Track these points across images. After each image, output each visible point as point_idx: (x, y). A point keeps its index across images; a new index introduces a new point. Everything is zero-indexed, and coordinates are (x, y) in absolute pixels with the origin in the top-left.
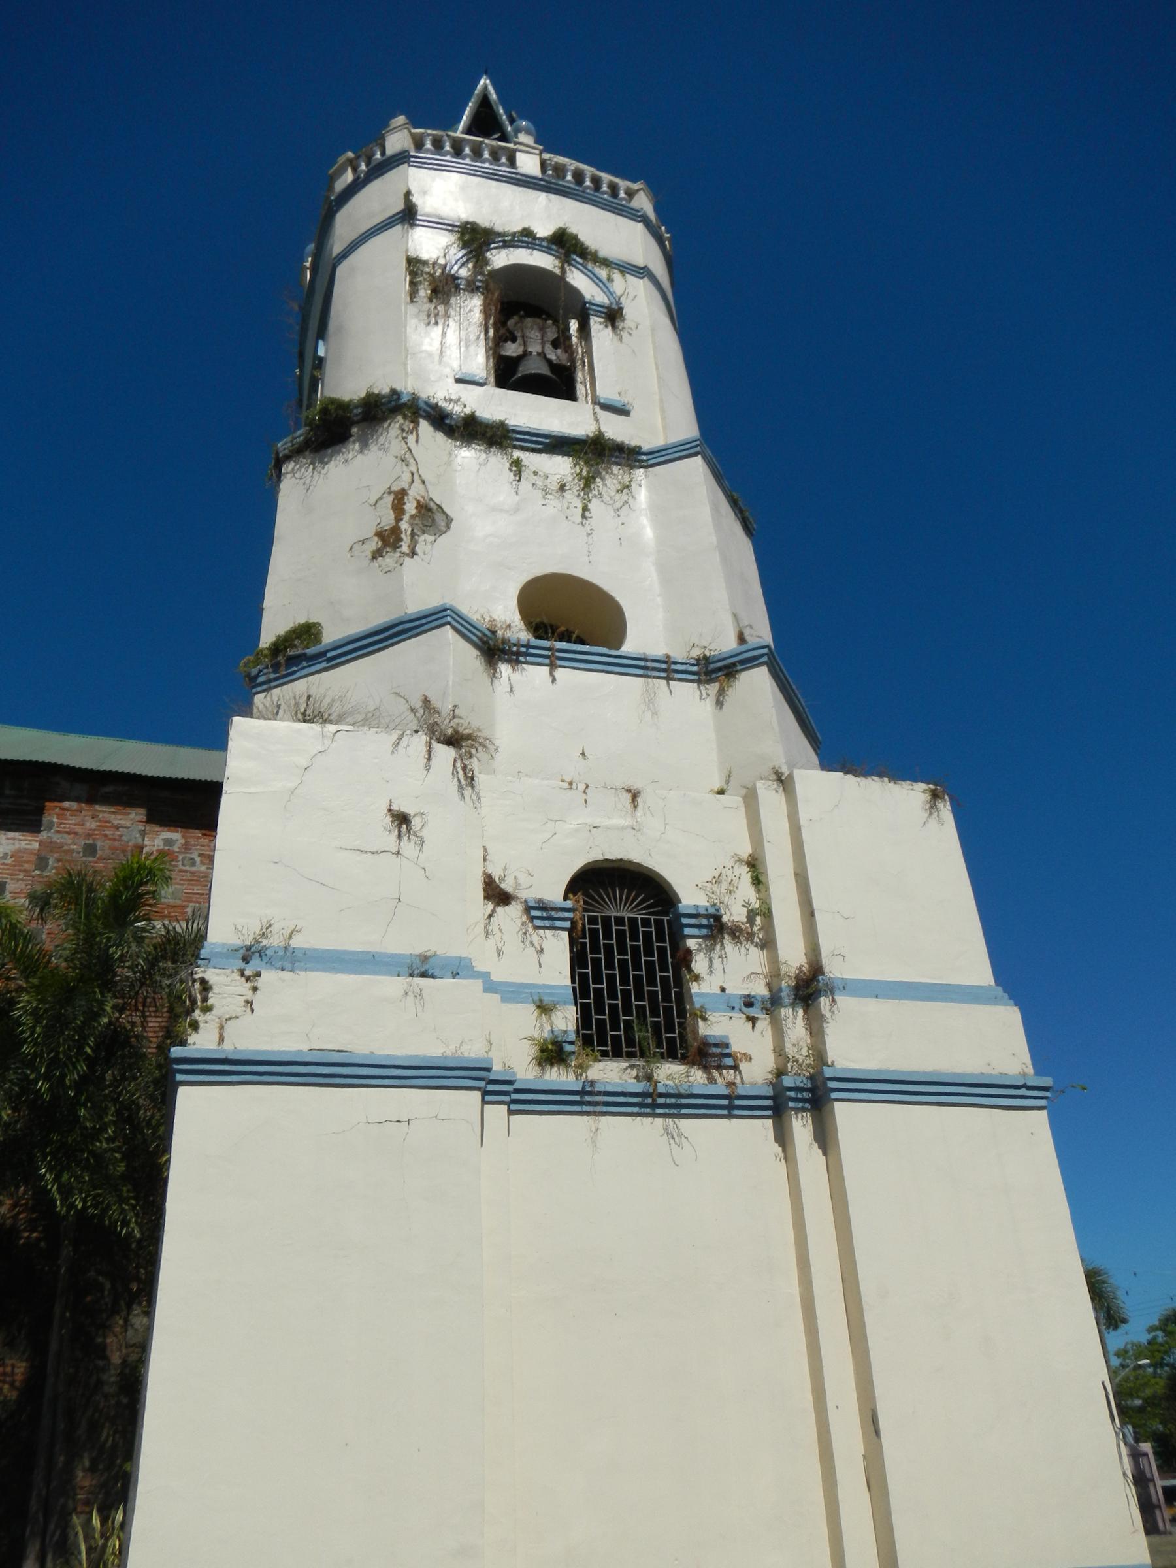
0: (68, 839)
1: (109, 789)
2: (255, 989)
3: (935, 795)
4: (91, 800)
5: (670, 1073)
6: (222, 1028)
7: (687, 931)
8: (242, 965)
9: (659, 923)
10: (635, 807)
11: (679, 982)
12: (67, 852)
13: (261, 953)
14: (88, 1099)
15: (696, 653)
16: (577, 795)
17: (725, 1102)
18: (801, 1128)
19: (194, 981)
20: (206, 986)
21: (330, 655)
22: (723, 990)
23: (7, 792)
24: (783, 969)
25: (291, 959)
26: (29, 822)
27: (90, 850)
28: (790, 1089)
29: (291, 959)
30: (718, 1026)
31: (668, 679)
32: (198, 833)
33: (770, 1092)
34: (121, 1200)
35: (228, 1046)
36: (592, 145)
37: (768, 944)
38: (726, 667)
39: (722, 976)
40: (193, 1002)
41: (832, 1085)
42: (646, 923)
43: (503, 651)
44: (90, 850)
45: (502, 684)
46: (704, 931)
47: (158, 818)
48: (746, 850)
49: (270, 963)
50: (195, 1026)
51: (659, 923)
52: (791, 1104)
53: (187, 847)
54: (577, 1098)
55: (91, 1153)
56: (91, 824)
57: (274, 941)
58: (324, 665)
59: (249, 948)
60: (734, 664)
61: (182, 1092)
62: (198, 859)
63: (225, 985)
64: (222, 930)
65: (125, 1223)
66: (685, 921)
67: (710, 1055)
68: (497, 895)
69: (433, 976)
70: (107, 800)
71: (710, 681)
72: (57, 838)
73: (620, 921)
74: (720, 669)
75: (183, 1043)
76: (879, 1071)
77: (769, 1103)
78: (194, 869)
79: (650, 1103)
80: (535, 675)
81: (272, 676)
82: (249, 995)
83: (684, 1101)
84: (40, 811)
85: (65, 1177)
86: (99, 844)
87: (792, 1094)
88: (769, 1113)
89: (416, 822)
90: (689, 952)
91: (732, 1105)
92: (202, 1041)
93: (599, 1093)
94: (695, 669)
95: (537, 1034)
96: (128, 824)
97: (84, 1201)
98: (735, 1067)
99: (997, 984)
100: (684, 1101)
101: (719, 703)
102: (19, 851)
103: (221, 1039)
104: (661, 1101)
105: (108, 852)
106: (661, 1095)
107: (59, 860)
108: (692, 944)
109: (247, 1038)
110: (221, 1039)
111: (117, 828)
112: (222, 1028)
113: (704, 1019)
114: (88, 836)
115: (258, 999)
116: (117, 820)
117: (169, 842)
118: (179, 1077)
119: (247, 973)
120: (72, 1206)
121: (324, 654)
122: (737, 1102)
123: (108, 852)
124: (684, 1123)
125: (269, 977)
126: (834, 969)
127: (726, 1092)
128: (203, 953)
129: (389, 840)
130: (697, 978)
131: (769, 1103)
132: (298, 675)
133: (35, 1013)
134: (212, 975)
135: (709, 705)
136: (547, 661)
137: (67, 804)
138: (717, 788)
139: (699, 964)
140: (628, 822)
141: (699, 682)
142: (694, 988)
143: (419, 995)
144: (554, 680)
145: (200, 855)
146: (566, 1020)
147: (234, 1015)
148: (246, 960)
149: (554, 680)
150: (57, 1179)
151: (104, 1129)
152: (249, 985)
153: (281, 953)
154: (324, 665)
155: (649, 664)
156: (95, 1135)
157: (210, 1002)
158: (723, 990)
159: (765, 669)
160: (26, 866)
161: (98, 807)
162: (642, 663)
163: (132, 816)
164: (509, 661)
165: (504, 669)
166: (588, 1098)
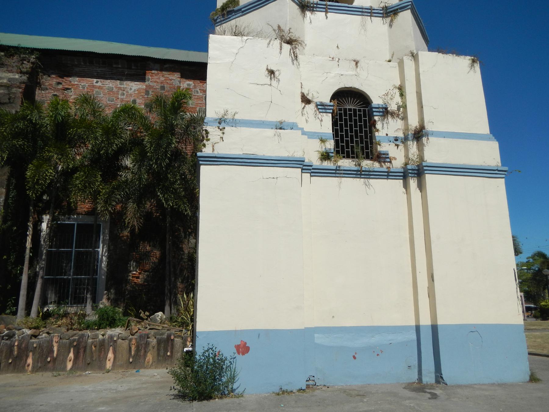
0: (155, 84)
2: (223, 133)
3: (474, 61)
4: (161, 70)
5: (367, 164)
6: (213, 146)
7: (375, 114)
8: (219, 125)
9: (364, 111)
11: (371, 132)
12: (155, 89)
14: (170, 172)
15: (382, 5)
16: (335, 63)
17: (386, 174)
18: (413, 183)
20: (207, 132)
21: (243, 10)
22: (387, 135)
23: (133, 67)
24: (410, 127)
25: (235, 123)
26: (141, 78)
27: (163, 88)
28: (410, 170)
29: (235, 123)
30: (384, 147)
31: (371, 16)
32: (198, 82)
33: (402, 171)
34: (184, 203)
35: (215, 152)
37: (405, 118)
38: (394, 10)
39: (386, 130)
40: (203, 137)
41: (425, 168)
42: (360, 111)
43: (308, 6)
44: (163, 88)
45: (307, 20)
46: (381, 114)
47: (185, 76)
48: (398, 83)
49: (228, 124)
50: (204, 145)
51: (364, 111)
52: (410, 175)
53: (195, 87)
54: (334, 172)
55: (173, 188)
56: (162, 79)
57: (229, 117)
58: (241, 14)
59: (220, 119)
60: (397, 9)
61: (202, 167)
62: (199, 91)
63: (213, 132)
64: (211, 113)
65: (186, 211)
66: (374, 110)
67: (381, 158)
68: (306, 100)
69: (284, 129)
70: (167, 70)
71: (387, 17)
72: (151, 84)
73: (350, 110)
74: (391, 12)
75: (201, 151)
76: (443, 164)
77: (402, 174)
79: (360, 173)
80: (320, 15)
81: (222, 19)
83: (371, 173)
84: (145, 74)
85: (166, 196)
86: (165, 86)
87: (411, 171)
88: (402, 178)
89: (277, 73)
90: (375, 121)
91: (388, 175)
92: (207, 151)
93: (342, 170)
94: (382, 12)
95: (320, 150)
96: (175, 78)
97: (173, 203)
98: (390, 162)
99: (491, 133)
100: (371, 173)
101: (391, 26)
102: (139, 89)
104: (363, 173)
105: (169, 89)
106: (363, 171)
108: (376, 118)
109: (222, 150)
111: (171, 80)
112: (213, 146)
113: (380, 145)
114: (162, 83)
115: (225, 137)
116: (171, 77)
117: (189, 85)
118: (201, 162)
119: (220, 128)
120: (169, 205)
121: (240, 9)
122: (390, 174)
124: (371, 181)
125: (228, 129)
126: (429, 127)
127: (386, 170)
128: (205, 121)
129: (267, 80)
130: (378, 130)
131: (402, 174)
132: (231, 18)
133: (151, 142)
134: (209, 128)
135: (386, 26)
136: (324, 10)
137: (153, 72)
138: (388, 59)
139: (379, 126)
140: (354, 73)
141: (383, 17)
142: (377, 134)
143: (279, 136)
144: (327, 17)
146: (330, 145)
147: (216, 143)
148: (220, 123)
149: (327, 17)
150: (163, 196)
151: (176, 181)
152: (221, 132)
153: (231, 121)
154: (241, 14)
155: (364, 10)
156: (174, 183)
158: (387, 135)
159: (409, 11)
160: (142, 94)
161: (164, 72)
162: (361, 10)
164: (310, 10)
165: (308, 13)
166: (338, 172)
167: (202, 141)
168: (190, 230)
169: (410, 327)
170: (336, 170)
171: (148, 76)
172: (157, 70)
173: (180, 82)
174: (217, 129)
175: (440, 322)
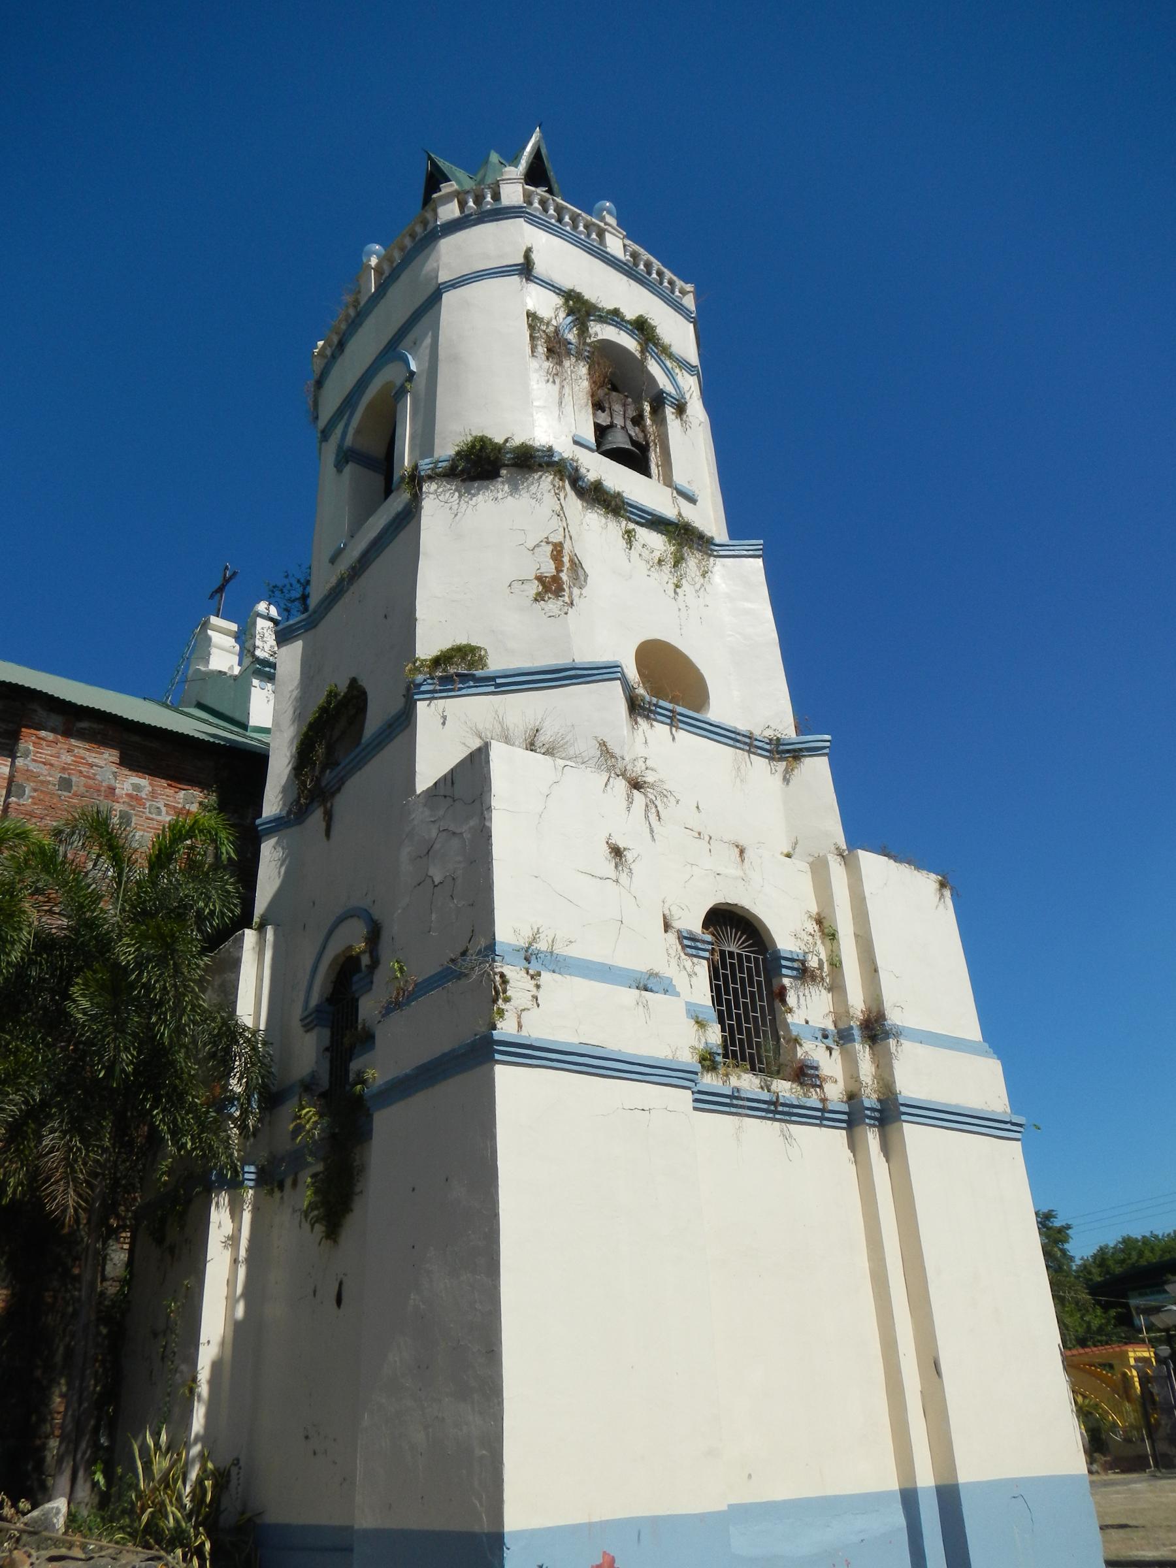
0: (44, 770)
1: (84, 725)
3: (942, 885)
4: (67, 733)
5: (784, 1088)
6: (519, 1017)
7: (784, 971)
8: (527, 965)
9: (756, 959)
10: (743, 861)
11: (772, 1011)
12: (42, 782)
13: (537, 954)
15: (769, 733)
16: (703, 844)
17: (819, 1114)
18: (872, 1139)
19: (495, 974)
21: (499, 681)
22: (807, 1022)
24: (851, 1011)
25: (560, 964)
27: (66, 784)
28: (868, 1109)
29: (560, 964)
30: (812, 1051)
31: (749, 752)
32: (164, 783)
33: (845, 1108)
35: (524, 1033)
36: (667, 240)
37: (837, 987)
38: (794, 750)
39: (808, 1010)
40: (497, 993)
41: (903, 1109)
42: (748, 959)
43: (644, 709)
44: (66, 784)
45: (640, 738)
46: (795, 973)
47: (130, 762)
48: (814, 909)
50: (501, 1012)
51: (756, 959)
52: (867, 1121)
53: (153, 795)
54: (727, 1101)
56: (67, 758)
57: (542, 945)
58: (492, 689)
60: (801, 750)
61: (498, 1068)
62: (164, 809)
66: (784, 963)
67: (804, 1074)
68: (667, 927)
69: (651, 991)
70: (82, 735)
71: (781, 759)
72: (33, 767)
73: (731, 954)
74: (788, 751)
76: (956, 1106)
77: (845, 1117)
78: (159, 818)
79: (774, 1110)
80: (661, 730)
81: (438, 688)
82: (534, 991)
83: (795, 1111)
84: (15, 737)
86: (74, 779)
87: (868, 1112)
88: (844, 1125)
89: (629, 855)
90: (783, 989)
91: (822, 1116)
93: (743, 1099)
94: (768, 747)
95: (696, 1044)
96: (102, 763)
98: (820, 1087)
99: (984, 1040)
100: (795, 1111)
101: (786, 780)
103: (520, 1026)
104: (780, 1109)
105: (82, 789)
106: (783, 1105)
107: (35, 790)
108: (786, 981)
110: (520, 1026)
111: (91, 766)
112: (519, 1017)
113: (801, 1045)
114: (64, 769)
115: (541, 995)
116: (92, 757)
117: (137, 787)
118: (498, 1057)
119: (531, 972)
121: (493, 678)
122: (827, 1115)
123: (82, 789)
124: (792, 1127)
125: (546, 977)
126: (894, 1017)
127: (820, 1106)
129: (607, 867)
130: (790, 1010)
131: (845, 1117)
132: (464, 692)
134: (507, 970)
135: (779, 777)
136: (668, 721)
137: (43, 733)
138: (785, 852)
139: (791, 999)
140: (740, 873)
141: (771, 759)
142: (790, 1018)
143: (646, 1006)
144: (674, 739)
145: (166, 805)
146: (714, 1036)
147: (535, 1010)
149: (674, 739)
152: (533, 982)
154: (492, 689)
155: (739, 737)
157: (509, 993)
158: (807, 1022)
159: (825, 759)
162: (733, 735)
163: (106, 756)
164: (648, 718)
165: (643, 723)
166: (735, 1102)
167: (495, 1001)
168: (114, 1223)
169: (888, 1494)
170: (823, 1110)
171: (28, 742)
172: (53, 730)
173: (115, 774)
174: (523, 973)
175: (965, 1476)
